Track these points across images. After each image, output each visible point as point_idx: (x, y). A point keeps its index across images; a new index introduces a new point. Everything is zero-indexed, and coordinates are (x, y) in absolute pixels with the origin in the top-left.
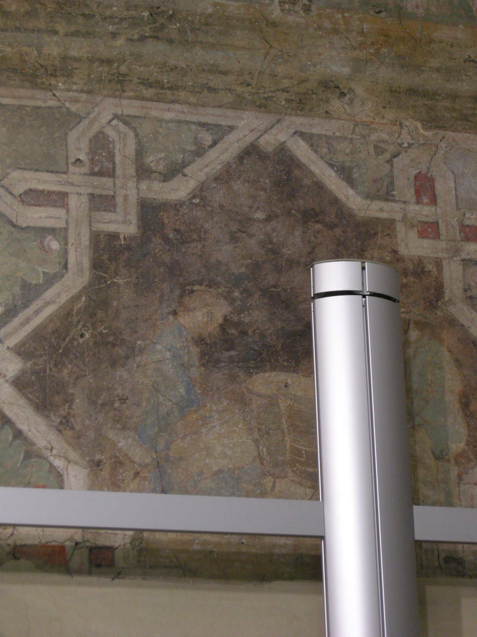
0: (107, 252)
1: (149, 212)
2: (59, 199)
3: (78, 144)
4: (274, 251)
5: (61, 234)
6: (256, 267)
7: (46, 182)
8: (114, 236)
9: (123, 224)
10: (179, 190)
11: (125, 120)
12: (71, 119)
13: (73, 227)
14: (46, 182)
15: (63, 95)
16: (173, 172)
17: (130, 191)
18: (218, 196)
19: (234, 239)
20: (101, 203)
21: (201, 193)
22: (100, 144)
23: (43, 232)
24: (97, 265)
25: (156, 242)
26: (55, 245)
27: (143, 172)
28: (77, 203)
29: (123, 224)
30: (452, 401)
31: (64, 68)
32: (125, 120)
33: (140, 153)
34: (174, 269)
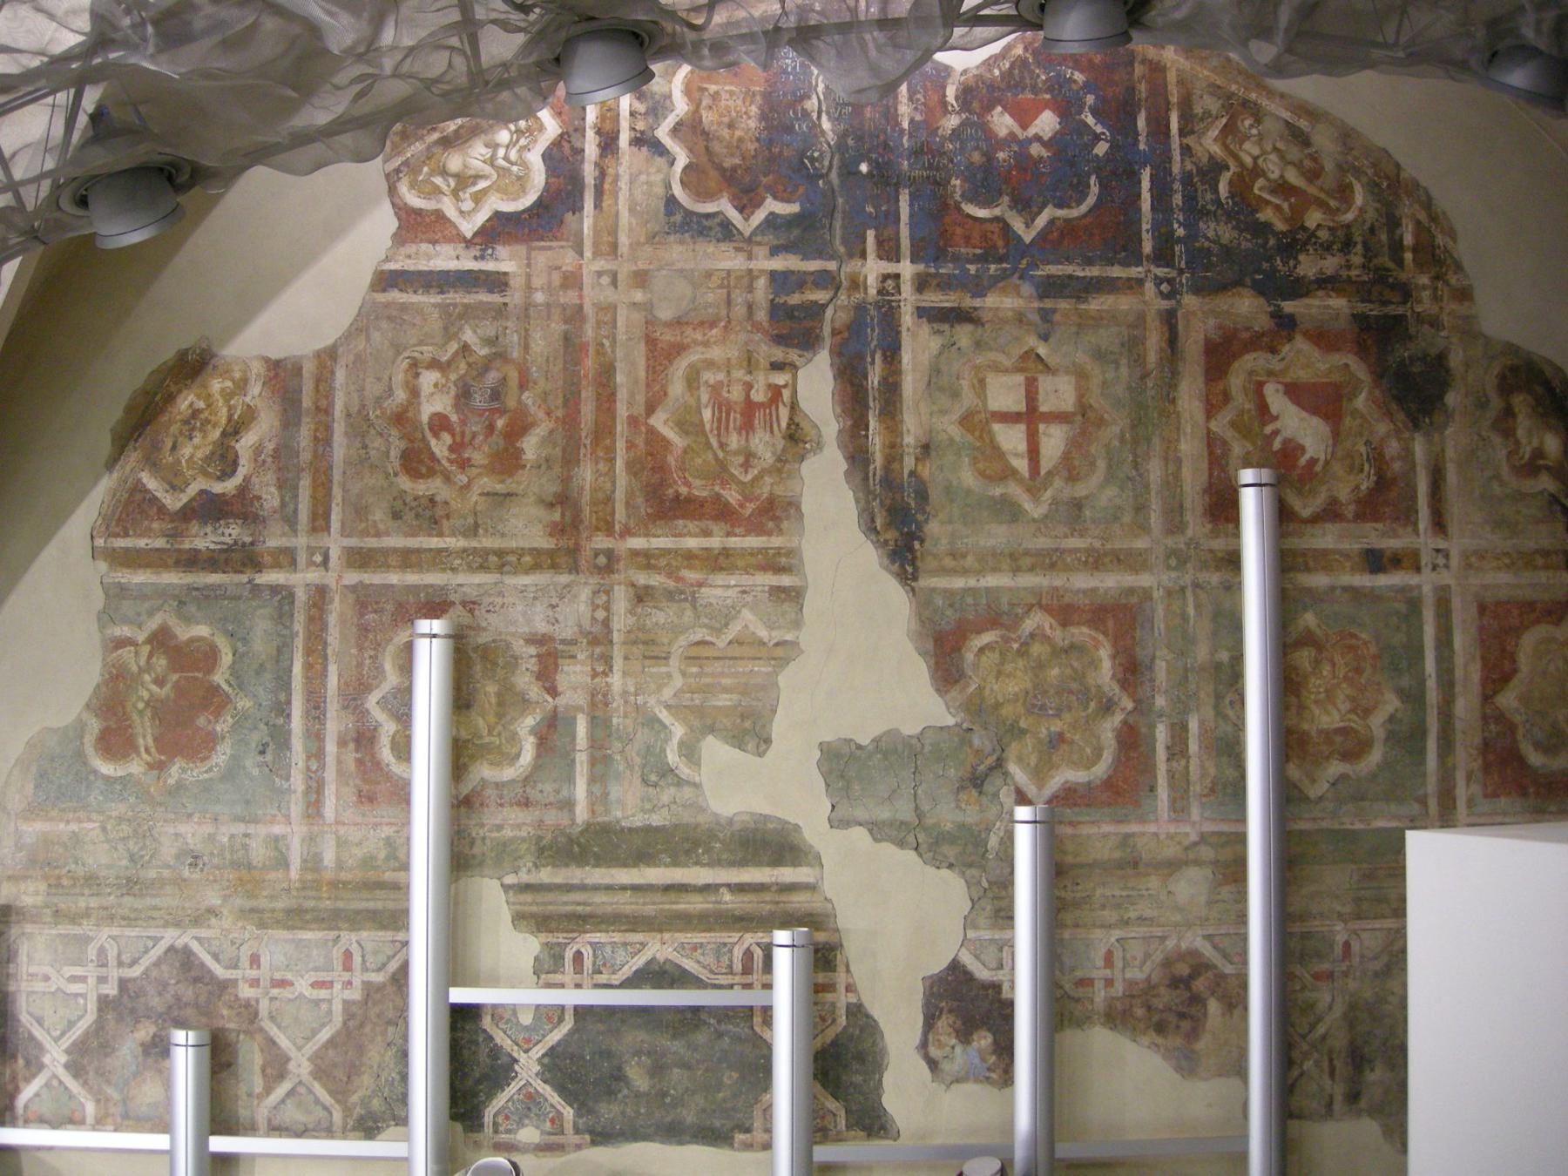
0: (104, 1003)
1: (123, 984)
2: (83, 979)
3: (92, 952)
4: (178, 999)
5: (84, 996)
6: (170, 1008)
7: (78, 971)
8: (107, 996)
9: (111, 990)
10: (136, 972)
11: (113, 938)
12: (87, 940)
13: (90, 991)
14: (78, 971)
15: (86, 928)
16: (134, 962)
17: (114, 974)
18: (154, 973)
19: (160, 994)
20: (102, 980)
21: (146, 973)
22: (102, 951)
23: (77, 995)
24: (100, 1010)
25: (125, 999)
26: (82, 1001)
27: (120, 964)
28: (92, 981)
29: (111, 990)
30: (257, 1069)
31: (87, 914)
32: (113, 938)
33: (119, 955)
34: (133, 1011)
